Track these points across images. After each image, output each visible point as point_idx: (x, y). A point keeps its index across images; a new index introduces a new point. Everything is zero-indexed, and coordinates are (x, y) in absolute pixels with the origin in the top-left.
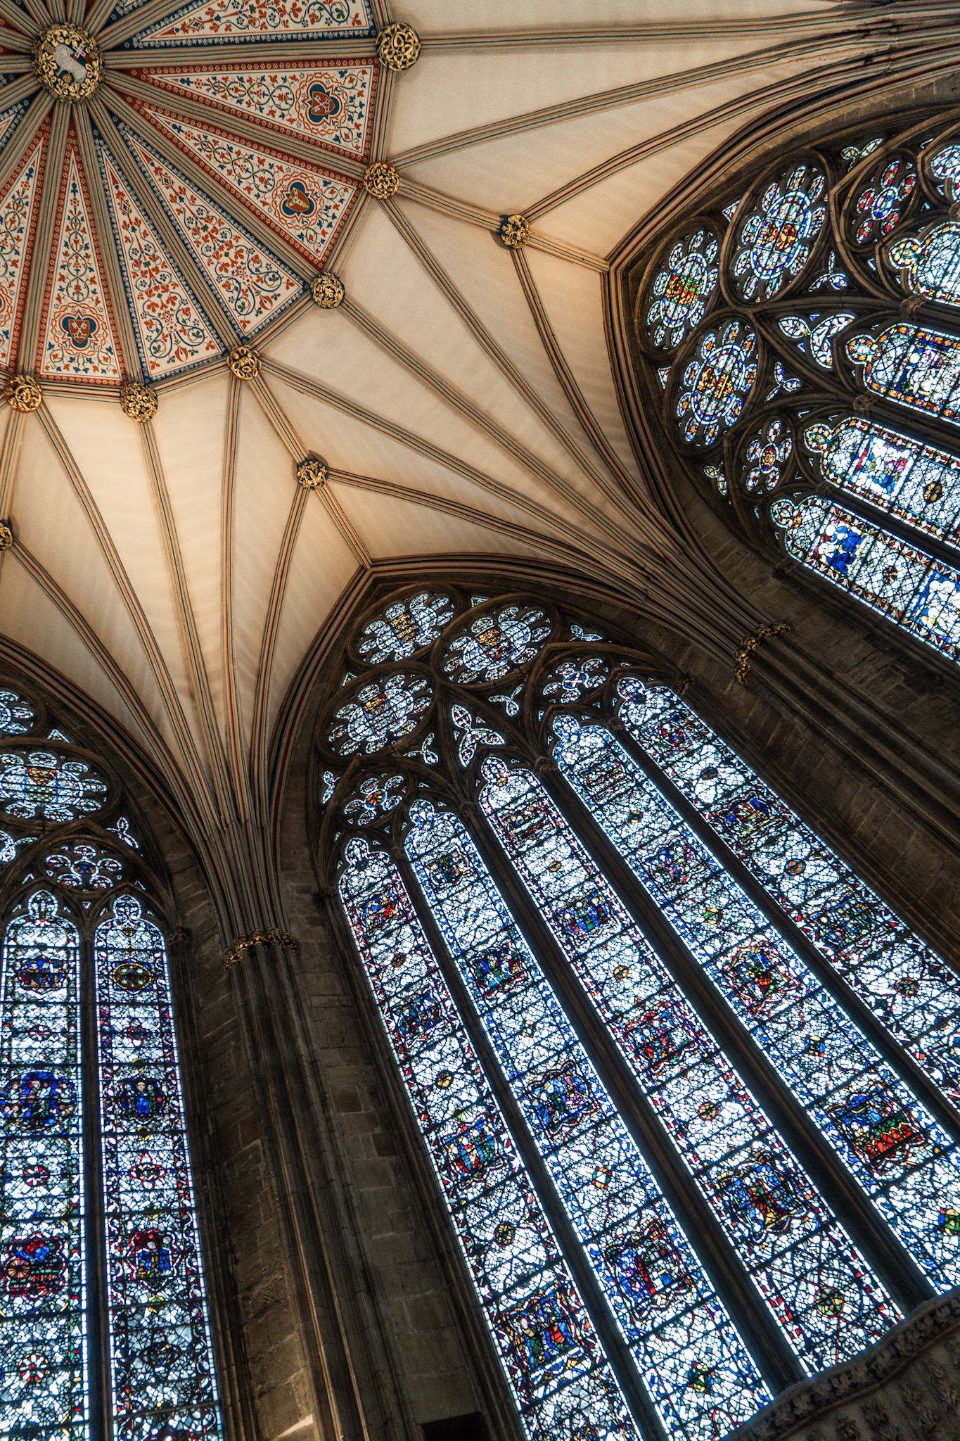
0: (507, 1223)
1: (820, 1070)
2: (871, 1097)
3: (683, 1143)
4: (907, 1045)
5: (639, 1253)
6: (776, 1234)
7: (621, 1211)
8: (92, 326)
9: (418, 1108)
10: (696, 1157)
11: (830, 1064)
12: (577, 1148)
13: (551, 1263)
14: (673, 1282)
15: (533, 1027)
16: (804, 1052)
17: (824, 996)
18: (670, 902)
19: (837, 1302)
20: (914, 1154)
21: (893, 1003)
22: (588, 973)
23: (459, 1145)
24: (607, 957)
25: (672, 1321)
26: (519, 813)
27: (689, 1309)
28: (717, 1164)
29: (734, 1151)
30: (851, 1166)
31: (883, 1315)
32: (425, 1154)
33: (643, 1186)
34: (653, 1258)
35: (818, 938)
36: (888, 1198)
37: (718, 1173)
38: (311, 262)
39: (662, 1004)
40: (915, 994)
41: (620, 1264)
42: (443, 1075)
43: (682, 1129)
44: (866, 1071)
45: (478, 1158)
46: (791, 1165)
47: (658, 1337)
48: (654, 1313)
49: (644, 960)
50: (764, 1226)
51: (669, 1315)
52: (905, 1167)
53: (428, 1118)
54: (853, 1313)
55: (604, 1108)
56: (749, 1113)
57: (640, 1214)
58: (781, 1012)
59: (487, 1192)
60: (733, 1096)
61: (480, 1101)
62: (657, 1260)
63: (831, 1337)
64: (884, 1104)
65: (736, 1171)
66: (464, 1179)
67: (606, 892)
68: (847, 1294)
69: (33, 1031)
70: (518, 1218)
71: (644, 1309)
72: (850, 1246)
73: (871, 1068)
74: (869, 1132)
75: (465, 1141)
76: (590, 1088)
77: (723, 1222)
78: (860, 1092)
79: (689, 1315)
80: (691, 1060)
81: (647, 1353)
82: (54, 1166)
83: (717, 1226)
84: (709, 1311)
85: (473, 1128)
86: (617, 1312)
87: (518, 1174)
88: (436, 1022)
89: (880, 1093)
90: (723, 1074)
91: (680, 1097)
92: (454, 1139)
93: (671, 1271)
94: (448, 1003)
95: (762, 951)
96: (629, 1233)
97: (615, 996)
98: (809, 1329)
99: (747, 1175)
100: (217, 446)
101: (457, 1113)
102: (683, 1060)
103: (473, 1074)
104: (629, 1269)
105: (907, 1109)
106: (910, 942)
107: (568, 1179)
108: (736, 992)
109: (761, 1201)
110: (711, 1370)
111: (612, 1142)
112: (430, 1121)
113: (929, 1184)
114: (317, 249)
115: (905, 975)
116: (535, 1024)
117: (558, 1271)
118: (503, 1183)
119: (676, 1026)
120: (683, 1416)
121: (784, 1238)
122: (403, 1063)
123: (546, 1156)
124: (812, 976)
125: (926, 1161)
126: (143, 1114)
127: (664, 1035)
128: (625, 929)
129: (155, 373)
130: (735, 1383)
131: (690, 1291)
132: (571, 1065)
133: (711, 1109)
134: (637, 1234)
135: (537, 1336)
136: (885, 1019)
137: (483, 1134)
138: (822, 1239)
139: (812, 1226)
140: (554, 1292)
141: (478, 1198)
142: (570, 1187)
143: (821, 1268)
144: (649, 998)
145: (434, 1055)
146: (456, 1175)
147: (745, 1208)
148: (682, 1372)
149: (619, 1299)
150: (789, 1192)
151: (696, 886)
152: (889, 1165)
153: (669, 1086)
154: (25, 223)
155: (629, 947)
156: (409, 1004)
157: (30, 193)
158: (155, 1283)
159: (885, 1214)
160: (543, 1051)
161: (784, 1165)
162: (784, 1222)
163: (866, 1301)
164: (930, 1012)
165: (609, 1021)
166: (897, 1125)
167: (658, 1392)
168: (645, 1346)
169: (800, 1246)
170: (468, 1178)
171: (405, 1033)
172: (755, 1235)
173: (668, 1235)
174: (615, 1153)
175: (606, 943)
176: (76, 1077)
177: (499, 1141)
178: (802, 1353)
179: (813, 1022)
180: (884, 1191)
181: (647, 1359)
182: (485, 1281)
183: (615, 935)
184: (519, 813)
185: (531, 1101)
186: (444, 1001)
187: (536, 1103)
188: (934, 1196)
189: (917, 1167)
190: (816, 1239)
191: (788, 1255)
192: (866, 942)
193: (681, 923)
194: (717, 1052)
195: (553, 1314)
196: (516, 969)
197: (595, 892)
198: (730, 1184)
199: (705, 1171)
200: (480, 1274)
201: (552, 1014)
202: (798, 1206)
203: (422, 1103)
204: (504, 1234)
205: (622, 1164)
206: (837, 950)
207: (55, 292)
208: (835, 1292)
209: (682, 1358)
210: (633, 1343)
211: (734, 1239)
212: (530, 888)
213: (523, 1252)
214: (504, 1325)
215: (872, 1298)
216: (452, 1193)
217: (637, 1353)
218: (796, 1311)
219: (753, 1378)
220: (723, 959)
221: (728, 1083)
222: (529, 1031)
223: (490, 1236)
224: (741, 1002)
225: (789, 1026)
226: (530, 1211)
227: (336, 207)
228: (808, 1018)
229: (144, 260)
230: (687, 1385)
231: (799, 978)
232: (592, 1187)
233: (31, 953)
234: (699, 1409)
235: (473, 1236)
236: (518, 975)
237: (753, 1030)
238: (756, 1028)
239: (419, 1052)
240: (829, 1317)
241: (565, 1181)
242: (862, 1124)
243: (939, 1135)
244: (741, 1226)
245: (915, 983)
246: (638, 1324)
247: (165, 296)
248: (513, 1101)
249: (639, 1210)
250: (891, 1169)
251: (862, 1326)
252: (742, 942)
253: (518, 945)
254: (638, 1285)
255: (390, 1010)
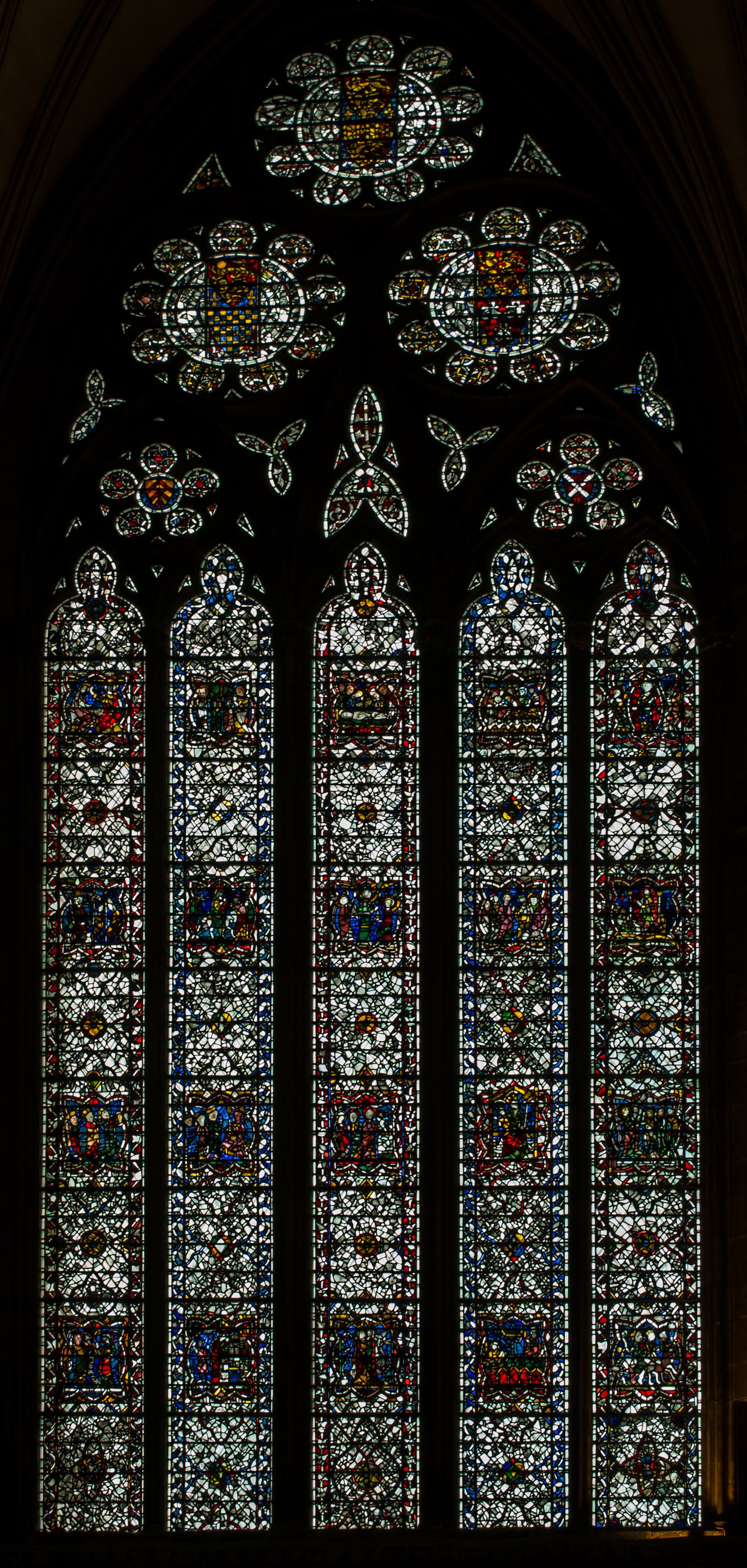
0: (101, 1234)
1: (501, 1273)
2: (528, 1328)
3: (322, 1260)
4: (599, 1301)
5: (222, 1339)
6: (357, 1396)
7: (225, 1290)
9: (49, 1042)
10: (327, 1282)
11: (514, 1273)
12: (211, 1201)
13: (128, 1299)
14: (239, 1384)
15: (229, 1025)
16: (498, 1245)
17: (561, 1199)
18: (474, 967)
19: (374, 1479)
20: (526, 1402)
21: (620, 1251)
22: (327, 998)
23: (81, 1118)
24: (361, 992)
25: (219, 1415)
26: (362, 685)
27: (240, 1414)
28: (343, 1302)
29: (366, 1299)
30: (465, 1379)
31: (404, 1509)
32: (38, 1106)
33: (259, 1280)
34: (232, 1351)
35: (603, 1130)
36: (476, 1424)
37: (339, 1311)
39: (391, 1094)
40: (647, 1257)
41: (197, 1340)
42: (95, 1017)
43: (331, 1247)
44: (543, 1301)
45: (96, 1145)
46: (411, 1345)
47: (200, 1421)
48: (207, 1399)
49: (400, 1026)
50: (351, 1383)
51: (221, 1409)
52: (509, 1408)
53: (56, 1062)
54: (381, 1494)
55: (261, 1175)
56: (404, 1272)
57: (241, 1306)
58: (507, 1187)
59: (92, 1189)
60: (400, 1246)
61: (125, 1080)
62: (235, 1356)
63: (351, 1502)
64: (535, 1342)
65: (358, 1317)
66: (71, 1159)
67: (410, 900)
68: (387, 1478)
70: (114, 1236)
71: (199, 1391)
72: (415, 1443)
74: (503, 1359)
75: (90, 1117)
76: (258, 1142)
77: (317, 1358)
78: (522, 1317)
79: (238, 1419)
80: (382, 1181)
81: (182, 1428)
83: (309, 1359)
84: (258, 1425)
85: (106, 1107)
86: (173, 1380)
87: (135, 1190)
88: (112, 941)
89: (539, 1330)
90: (404, 1216)
91: (348, 1213)
92: (76, 1106)
93: (242, 1372)
94: (138, 924)
95: (537, 1103)
96: (220, 1315)
97: (343, 1051)
98: (336, 1487)
99: (365, 1330)
101: (91, 1077)
102: (374, 1175)
103: (131, 1039)
104: (203, 1348)
105: (553, 1360)
106: (688, 1197)
107: (186, 1227)
108: (476, 1134)
109: (364, 1361)
110: (233, 1472)
111: (252, 1216)
112: (57, 1067)
113: (519, 1433)
115: (654, 1230)
116: (232, 1023)
117: (133, 1310)
118: (114, 1190)
119: (390, 1132)
120: (189, 1493)
121: (362, 1404)
122: (50, 970)
123: (175, 1190)
124: (566, 1168)
125: (532, 1413)
127: (370, 1133)
128: (403, 967)
130: (247, 1492)
131: (251, 1399)
132: (246, 1101)
133: (370, 1245)
134: (228, 1321)
135: (86, 1359)
136: (599, 1261)
137: (113, 1120)
138: (396, 1424)
139: (394, 1408)
140: (119, 1327)
141: (81, 1189)
142: (184, 1236)
143: (379, 1446)
144: (381, 1078)
145: (93, 987)
146: (65, 1149)
147: (344, 1358)
148: (206, 1460)
149: (180, 1370)
150: (393, 1368)
151: (519, 968)
152: (498, 1398)
153: (343, 1194)
155: (395, 996)
156: (87, 890)
159: (464, 1435)
160: (226, 1064)
161: (406, 1342)
162: (372, 1391)
163: (398, 1491)
164: (645, 1284)
165: (319, 1076)
166: (531, 1369)
167: (176, 1465)
168: (185, 1423)
169: (373, 1419)
170: (76, 1161)
171: (66, 929)
172: (337, 1385)
173: (258, 1339)
174: (248, 1230)
175: (370, 971)
177: (129, 1141)
178: (318, 1501)
179: (530, 1220)
180: (477, 1417)
181: (181, 1434)
182: (54, 1278)
183: (386, 968)
184: (362, 685)
185: (185, 1116)
186: (133, 917)
187: (189, 1122)
188: (516, 1446)
189: (521, 1415)
190: (391, 1421)
191: (357, 1420)
192: (646, 1168)
193: (471, 1005)
194: (414, 1189)
195: (110, 1347)
196: (244, 933)
197: (397, 889)
198: (344, 1327)
199: (328, 1302)
200: (52, 1269)
201: (258, 1024)
202: (393, 1384)
203: (56, 1039)
204: (93, 1244)
205: (250, 1245)
206: (613, 1155)
208: (378, 1471)
209: (213, 1449)
210: (174, 1414)
211: (318, 1379)
212: (319, 824)
213: (106, 1273)
214: (57, 1331)
215: (404, 1492)
216: (53, 1167)
217: (174, 1424)
218: (334, 1467)
219: (265, 1497)
220: (489, 1085)
221: (404, 1228)
222: (222, 1028)
223: (77, 1237)
224: (473, 1149)
225: (504, 1208)
226: (130, 1236)
228: (529, 1211)
230: (205, 1473)
231: (552, 1162)
232: (206, 1250)
234: (205, 1495)
235: (59, 1227)
236: (243, 942)
237: (466, 1189)
238: (470, 1187)
239: (74, 970)
240: (359, 1487)
241: (181, 1227)
242: (501, 1348)
243: (561, 1398)
244: (331, 1372)
245: (657, 1245)
246: (187, 1401)
248: (164, 1106)
249: (242, 1300)
250: (497, 1402)
251: (381, 1509)
252: (522, 1077)
253: (262, 900)
254: (205, 1368)
255: (58, 881)
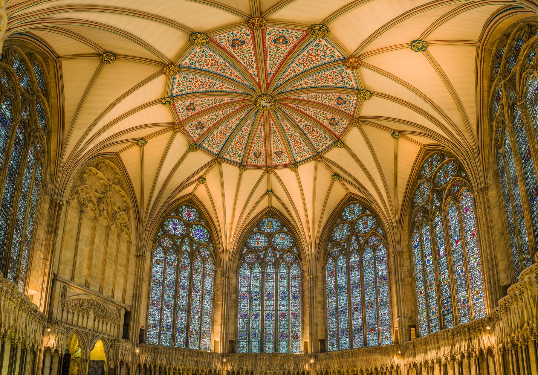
8: (282, 152)
38: (336, 136)
69: (282, 286)
73: (375, 322)
82: (285, 305)
100: (312, 176)
114: (338, 134)
126: (296, 298)
129: (297, 161)
154: (263, 135)
157: (262, 129)
158: (295, 319)
176: (288, 293)
207: (272, 147)
227: (344, 125)
229: (293, 136)
233: (282, 274)
247: (298, 144)
